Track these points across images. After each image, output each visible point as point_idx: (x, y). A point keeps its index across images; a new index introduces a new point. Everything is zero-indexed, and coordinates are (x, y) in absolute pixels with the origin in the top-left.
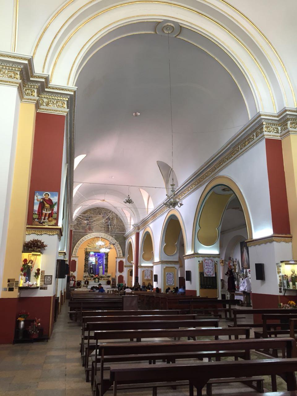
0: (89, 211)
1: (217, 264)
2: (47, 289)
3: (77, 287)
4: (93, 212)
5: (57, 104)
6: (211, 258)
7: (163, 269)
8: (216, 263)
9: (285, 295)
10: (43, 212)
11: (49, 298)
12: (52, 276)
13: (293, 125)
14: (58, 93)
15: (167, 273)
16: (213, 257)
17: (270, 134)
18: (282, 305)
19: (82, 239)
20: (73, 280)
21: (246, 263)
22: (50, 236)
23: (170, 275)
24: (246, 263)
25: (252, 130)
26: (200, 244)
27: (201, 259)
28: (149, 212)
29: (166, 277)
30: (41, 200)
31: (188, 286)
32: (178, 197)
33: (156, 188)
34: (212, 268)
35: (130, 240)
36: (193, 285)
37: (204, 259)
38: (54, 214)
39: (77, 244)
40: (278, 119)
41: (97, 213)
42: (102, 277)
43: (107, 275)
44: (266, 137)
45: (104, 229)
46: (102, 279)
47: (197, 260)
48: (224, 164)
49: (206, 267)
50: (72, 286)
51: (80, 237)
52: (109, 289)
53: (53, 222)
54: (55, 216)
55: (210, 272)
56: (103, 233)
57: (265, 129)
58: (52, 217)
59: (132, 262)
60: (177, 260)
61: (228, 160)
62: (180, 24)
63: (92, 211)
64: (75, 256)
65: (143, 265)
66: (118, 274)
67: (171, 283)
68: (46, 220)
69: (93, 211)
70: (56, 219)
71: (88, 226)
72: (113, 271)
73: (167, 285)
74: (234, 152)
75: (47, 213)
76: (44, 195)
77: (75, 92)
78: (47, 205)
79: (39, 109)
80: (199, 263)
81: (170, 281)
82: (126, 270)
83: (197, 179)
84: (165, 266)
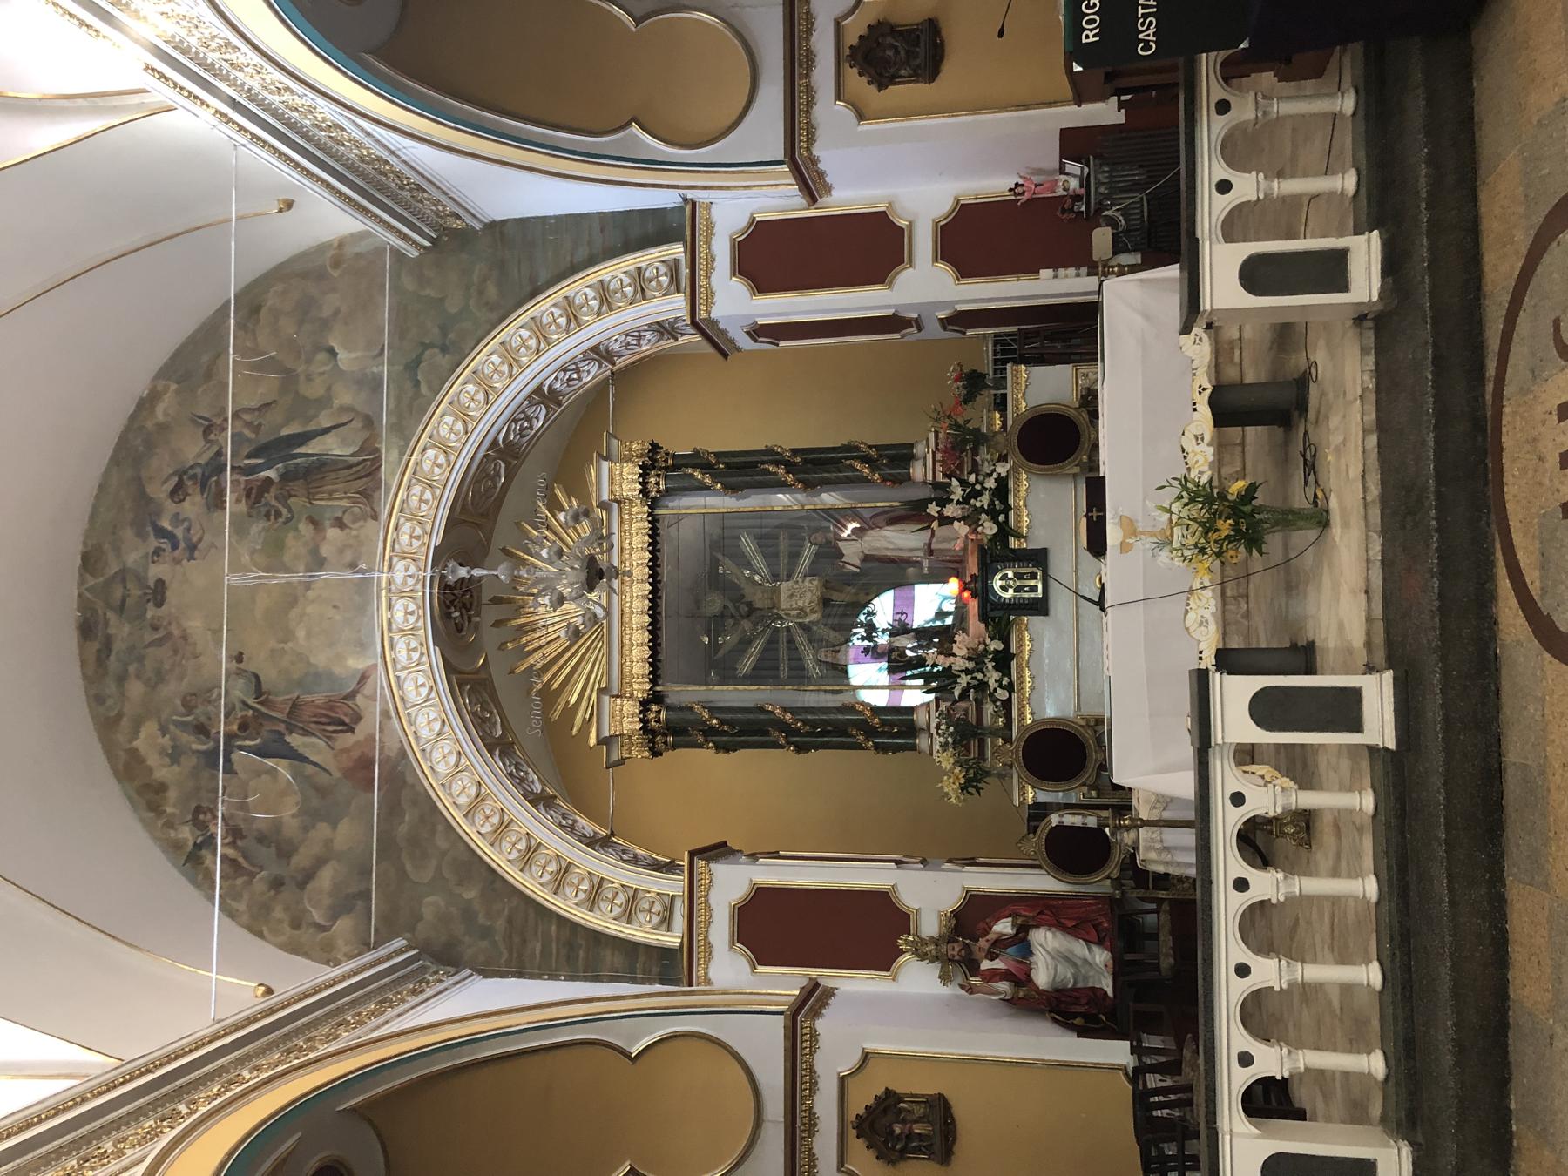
0: (121, 737)
3: (1089, 774)
4: (135, 689)
19: (456, 817)
20: (1020, 939)
39: (533, 884)
41: (149, 636)
45: (332, 533)
50: (1101, 956)
51: (441, 843)
52: (1222, 285)
64: (680, 911)
66: (925, 284)
69: (122, 679)
71: (295, 740)
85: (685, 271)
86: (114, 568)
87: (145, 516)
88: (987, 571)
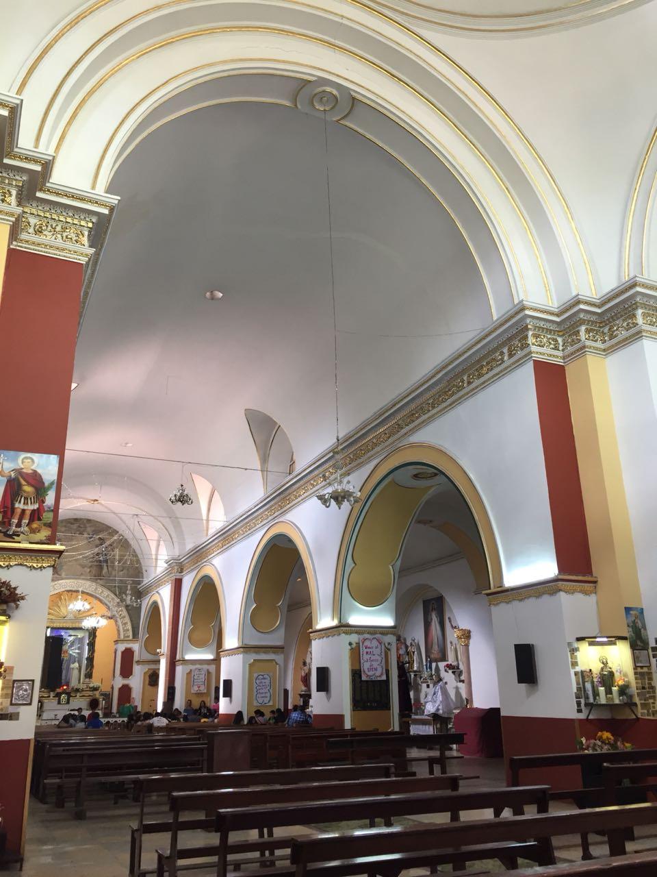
1: (389, 650)
2: (17, 719)
5: (65, 234)
6: (377, 636)
7: (248, 666)
8: (389, 647)
9: (589, 718)
10: (17, 505)
11: (24, 743)
12: (33, 681)
13: (591, 334)
14: (68, 208)
15: (255, 675)
16: (380, 633)
17: (542, 350)
18: (584, 742)
21: (435, 647)
22: (34, 571)
23: (263, 680)
24: (435, 647)
25: (501, 340)
26: (354, 601)
27: (354, 638)
28: (212, 531)
29: (255, 685)
30: (13, 475)
31: (319, 705)
32: (295, 493)
33: (246, 469)
34: (379, 658)
35: (156, 598)
36: (335, 703)
37: (362, 637)
38: (44, 512)
40: (558, 319)
42: (77, 690)
43: (91, 685)
44: (536, 357)
45: (89, 570)
46: (78, 694)
47: (345, 639)
48: (424, 417)
49: (366, 657)
53: (44, 533)
54: (48, 517)
55: (376, 669)
56: (87, 580)
57: (531, 340)
58: (40, 519)
59: (158, 650)
60: (279, 643)
61: (433, 407)
62: (352, 93)
63: (62, 527)
65: (188, 657)
66: (119, 682)
67: (266, 700)
68: (24, 528)
69: (65, 526)
70: (50, 527)
72: (106, 676)
73: (255, 703)
74: (449, 390)
75: (26, 507)
76: (20, 462)
77: (112, 209)
78: (28, 488)
79: (15, 240)
80: (349, 647)
81: (262, 695)
82: (139, 672)
83: (350, 451)
84: (252, 657)
85: (128, 639)
86: (88, 525)
87: (96, 532)
88: (67, 693)
